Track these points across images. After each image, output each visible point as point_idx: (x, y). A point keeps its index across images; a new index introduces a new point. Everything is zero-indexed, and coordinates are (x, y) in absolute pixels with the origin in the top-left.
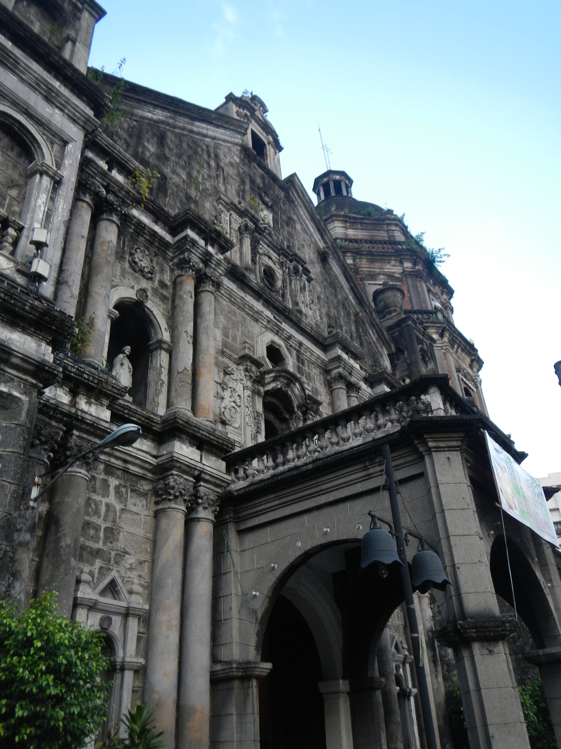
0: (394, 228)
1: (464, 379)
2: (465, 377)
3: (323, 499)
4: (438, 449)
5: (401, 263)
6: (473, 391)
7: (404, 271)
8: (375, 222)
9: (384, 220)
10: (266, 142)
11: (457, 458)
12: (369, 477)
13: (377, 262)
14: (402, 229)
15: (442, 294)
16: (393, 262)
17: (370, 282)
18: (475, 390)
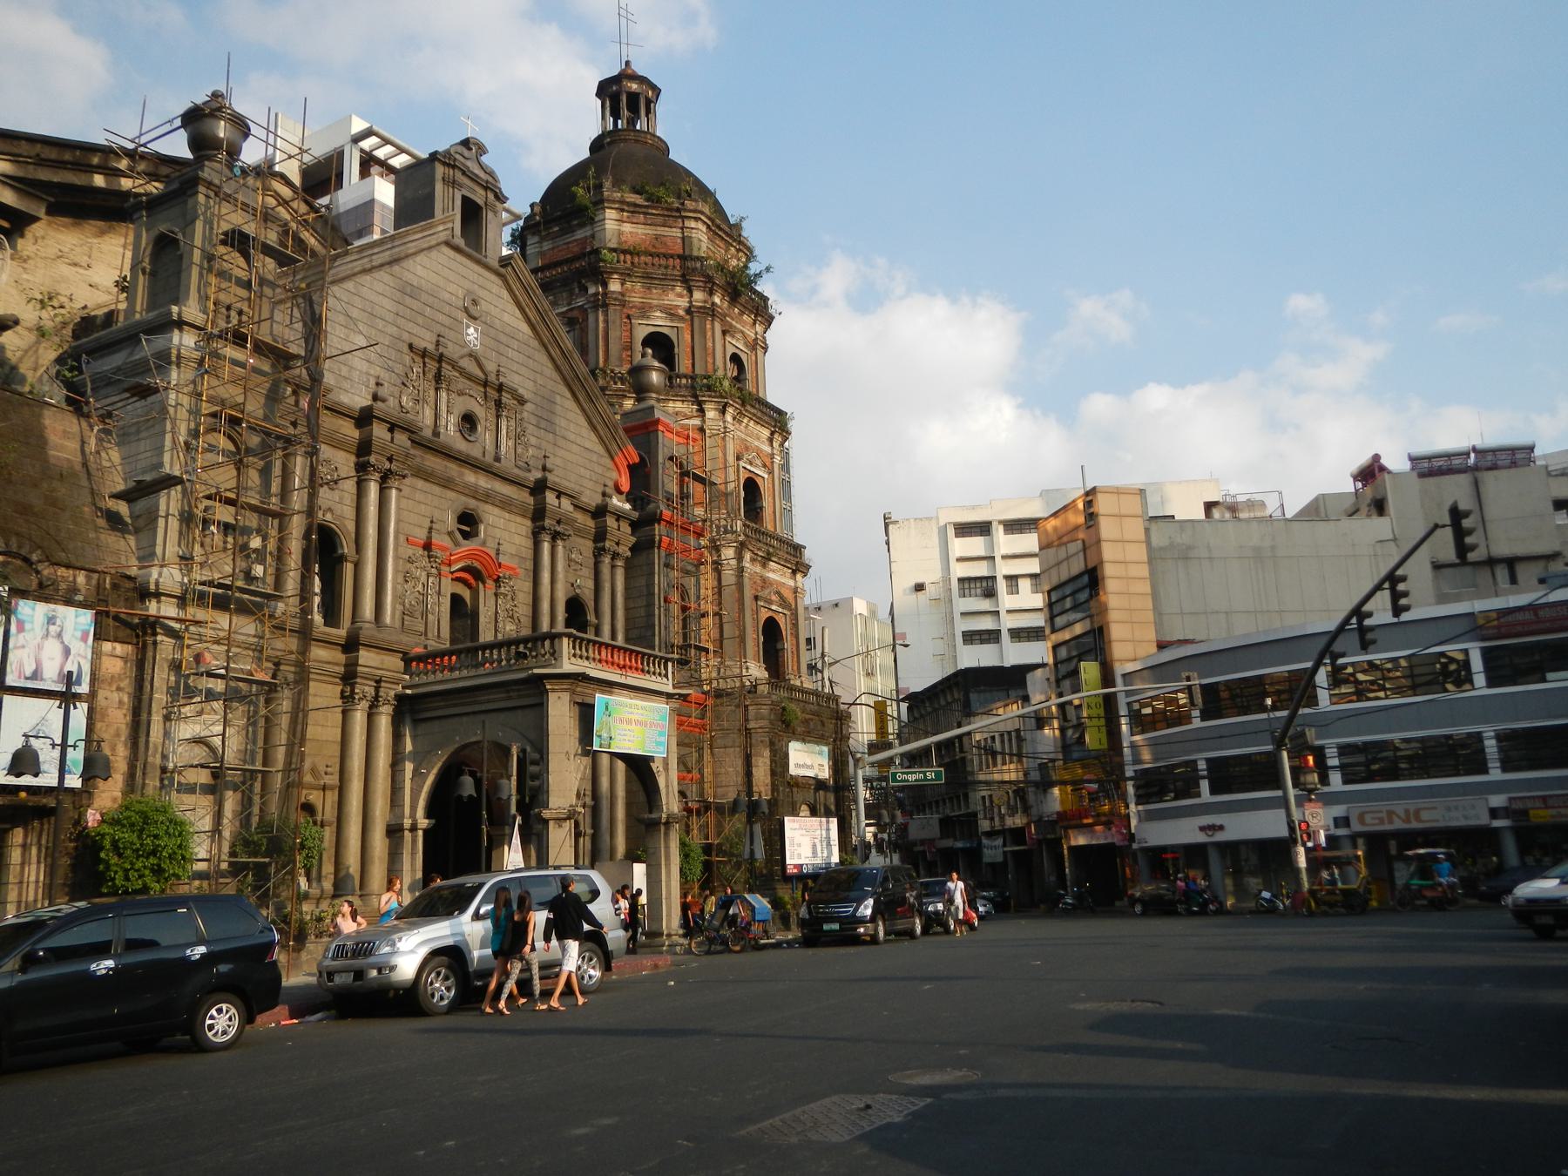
0: (693, 224)
1: (749, 467)
2: (751, 464)
3: (477, 708)
4: (553, 690)
5: (690, 292)
7: (690, 307)
8: (666, 213)
9: (678, 210)
10: (480, 202)
11: (566, 697)
12: (510, 698)
13: (656, 288)
14: (705, 223)
15: (754, 324)
16: (678, 289)
18: (766, 476)
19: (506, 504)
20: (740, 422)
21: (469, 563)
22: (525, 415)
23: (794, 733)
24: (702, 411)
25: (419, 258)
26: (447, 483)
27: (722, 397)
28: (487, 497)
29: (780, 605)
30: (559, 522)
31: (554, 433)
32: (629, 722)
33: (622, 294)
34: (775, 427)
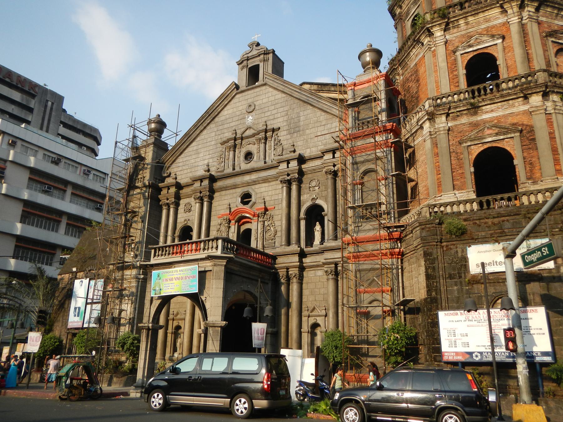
1: (471, 49)
2: (470, 46)
6: (497, 44)
17: (407, 19)
19: (266, 180)
20: (458, 26)
21: (240, 215)
22: (279, 135)
23: (473, 239)
24: (423, 44)
25: (226, 109)
26: (235, 187)
27: (422, 28)
28: (255, 182)
29: (497, 134)
30: (288, 175)
31: (299, 131)
32: (171, 279)
33: (399, 13)
34: (498, 3)
